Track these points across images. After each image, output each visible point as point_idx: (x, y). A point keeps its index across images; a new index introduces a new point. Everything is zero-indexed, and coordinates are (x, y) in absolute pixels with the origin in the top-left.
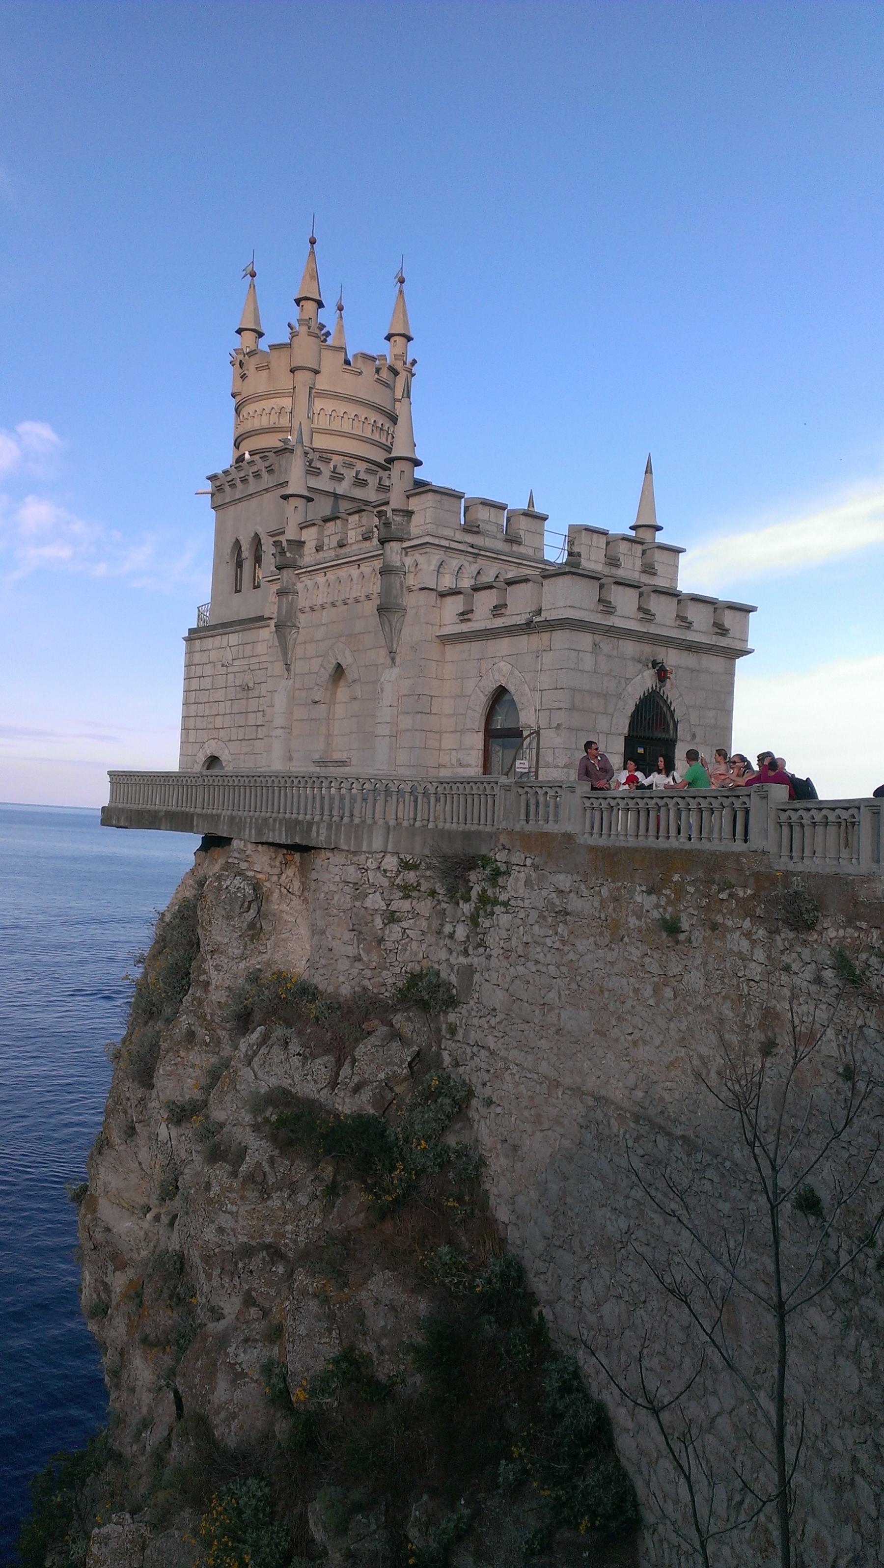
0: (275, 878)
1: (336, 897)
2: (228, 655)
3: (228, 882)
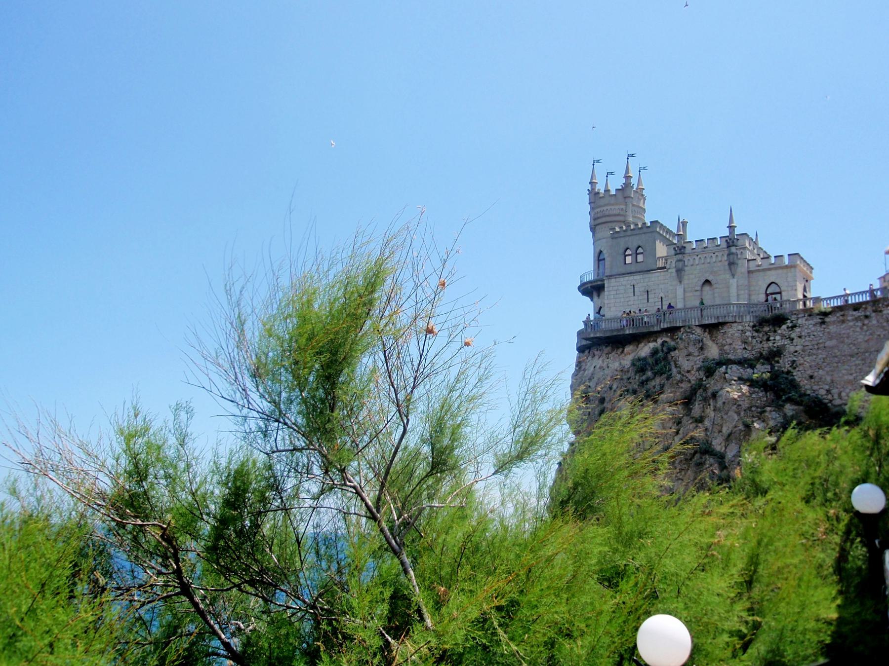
2: (634, 282)
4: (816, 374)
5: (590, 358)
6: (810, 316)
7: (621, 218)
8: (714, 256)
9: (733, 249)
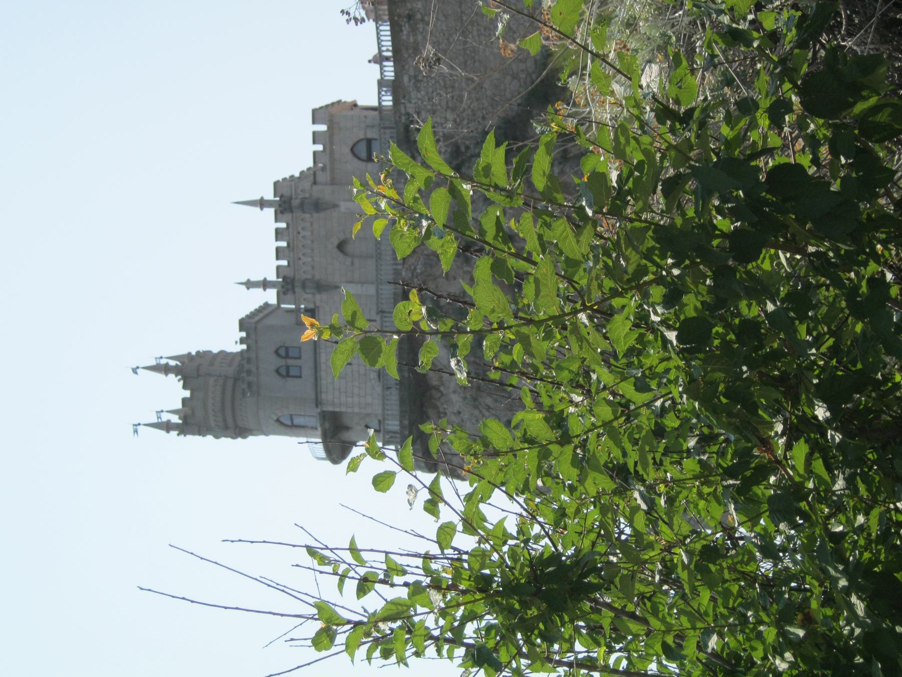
3: (419, 271)
4: (489, 93)
6: (404, 97)
7: (230, 383)
8: (303, 233)
9: (295, 203)
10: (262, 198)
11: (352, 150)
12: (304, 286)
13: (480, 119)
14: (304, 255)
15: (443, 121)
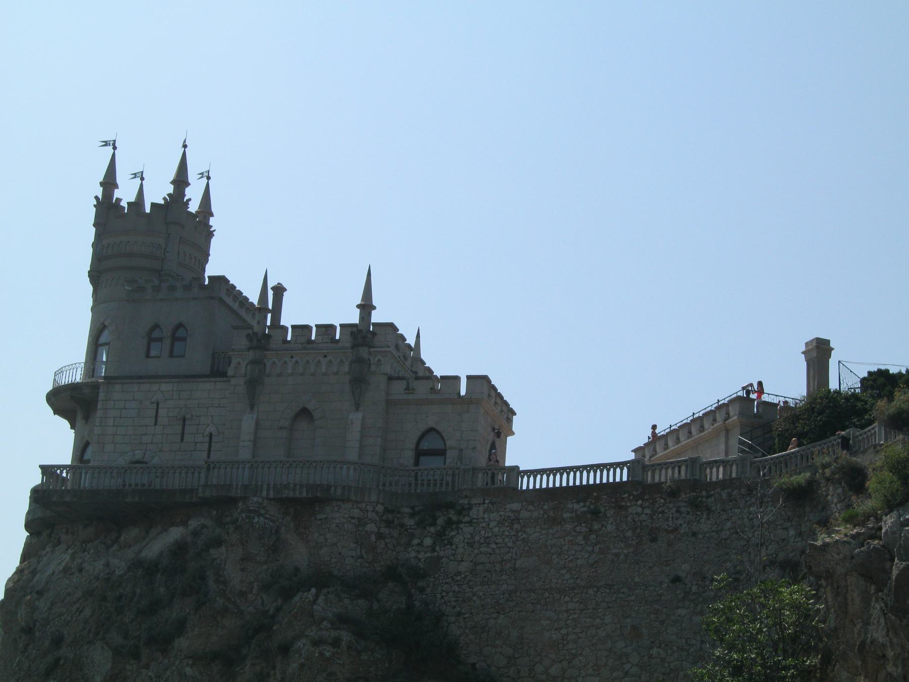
0: (280, 520)
1: (346, 526)
3: (256, 520)
5: (48, 549)
6: (492, 503)
9: (363, 352)
10: (374, 308)
11: (432, 430)
12: (254, 362)
13: (458, 609)
14: (297, 362)
15: (459, 558)
